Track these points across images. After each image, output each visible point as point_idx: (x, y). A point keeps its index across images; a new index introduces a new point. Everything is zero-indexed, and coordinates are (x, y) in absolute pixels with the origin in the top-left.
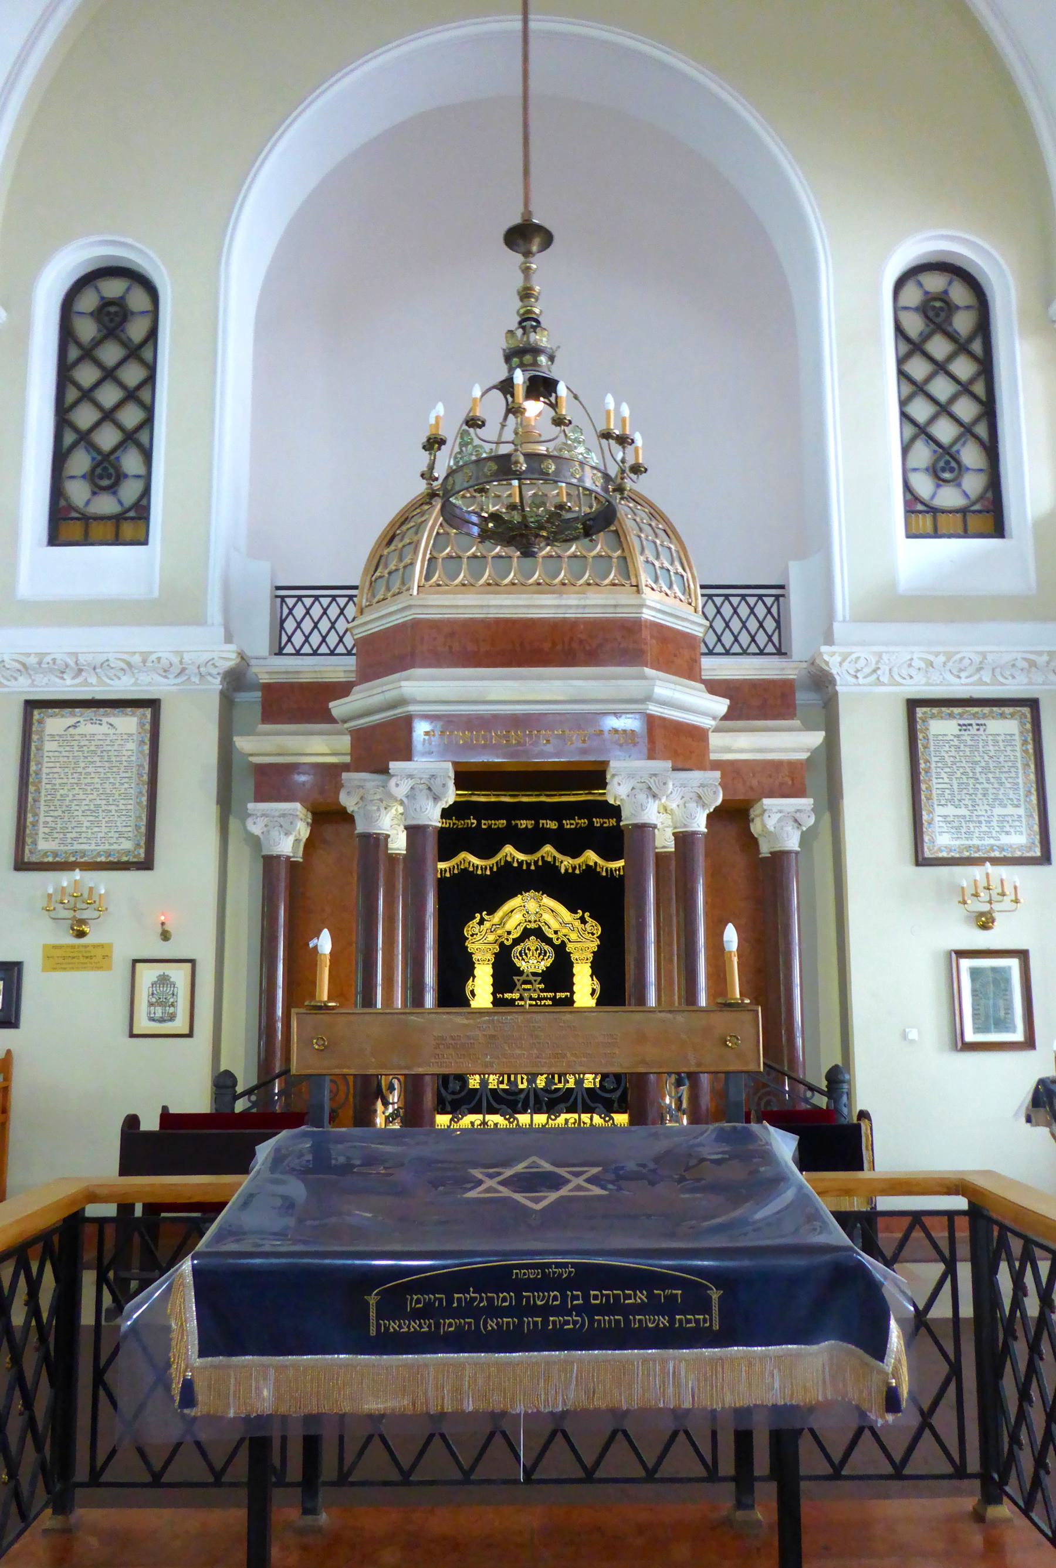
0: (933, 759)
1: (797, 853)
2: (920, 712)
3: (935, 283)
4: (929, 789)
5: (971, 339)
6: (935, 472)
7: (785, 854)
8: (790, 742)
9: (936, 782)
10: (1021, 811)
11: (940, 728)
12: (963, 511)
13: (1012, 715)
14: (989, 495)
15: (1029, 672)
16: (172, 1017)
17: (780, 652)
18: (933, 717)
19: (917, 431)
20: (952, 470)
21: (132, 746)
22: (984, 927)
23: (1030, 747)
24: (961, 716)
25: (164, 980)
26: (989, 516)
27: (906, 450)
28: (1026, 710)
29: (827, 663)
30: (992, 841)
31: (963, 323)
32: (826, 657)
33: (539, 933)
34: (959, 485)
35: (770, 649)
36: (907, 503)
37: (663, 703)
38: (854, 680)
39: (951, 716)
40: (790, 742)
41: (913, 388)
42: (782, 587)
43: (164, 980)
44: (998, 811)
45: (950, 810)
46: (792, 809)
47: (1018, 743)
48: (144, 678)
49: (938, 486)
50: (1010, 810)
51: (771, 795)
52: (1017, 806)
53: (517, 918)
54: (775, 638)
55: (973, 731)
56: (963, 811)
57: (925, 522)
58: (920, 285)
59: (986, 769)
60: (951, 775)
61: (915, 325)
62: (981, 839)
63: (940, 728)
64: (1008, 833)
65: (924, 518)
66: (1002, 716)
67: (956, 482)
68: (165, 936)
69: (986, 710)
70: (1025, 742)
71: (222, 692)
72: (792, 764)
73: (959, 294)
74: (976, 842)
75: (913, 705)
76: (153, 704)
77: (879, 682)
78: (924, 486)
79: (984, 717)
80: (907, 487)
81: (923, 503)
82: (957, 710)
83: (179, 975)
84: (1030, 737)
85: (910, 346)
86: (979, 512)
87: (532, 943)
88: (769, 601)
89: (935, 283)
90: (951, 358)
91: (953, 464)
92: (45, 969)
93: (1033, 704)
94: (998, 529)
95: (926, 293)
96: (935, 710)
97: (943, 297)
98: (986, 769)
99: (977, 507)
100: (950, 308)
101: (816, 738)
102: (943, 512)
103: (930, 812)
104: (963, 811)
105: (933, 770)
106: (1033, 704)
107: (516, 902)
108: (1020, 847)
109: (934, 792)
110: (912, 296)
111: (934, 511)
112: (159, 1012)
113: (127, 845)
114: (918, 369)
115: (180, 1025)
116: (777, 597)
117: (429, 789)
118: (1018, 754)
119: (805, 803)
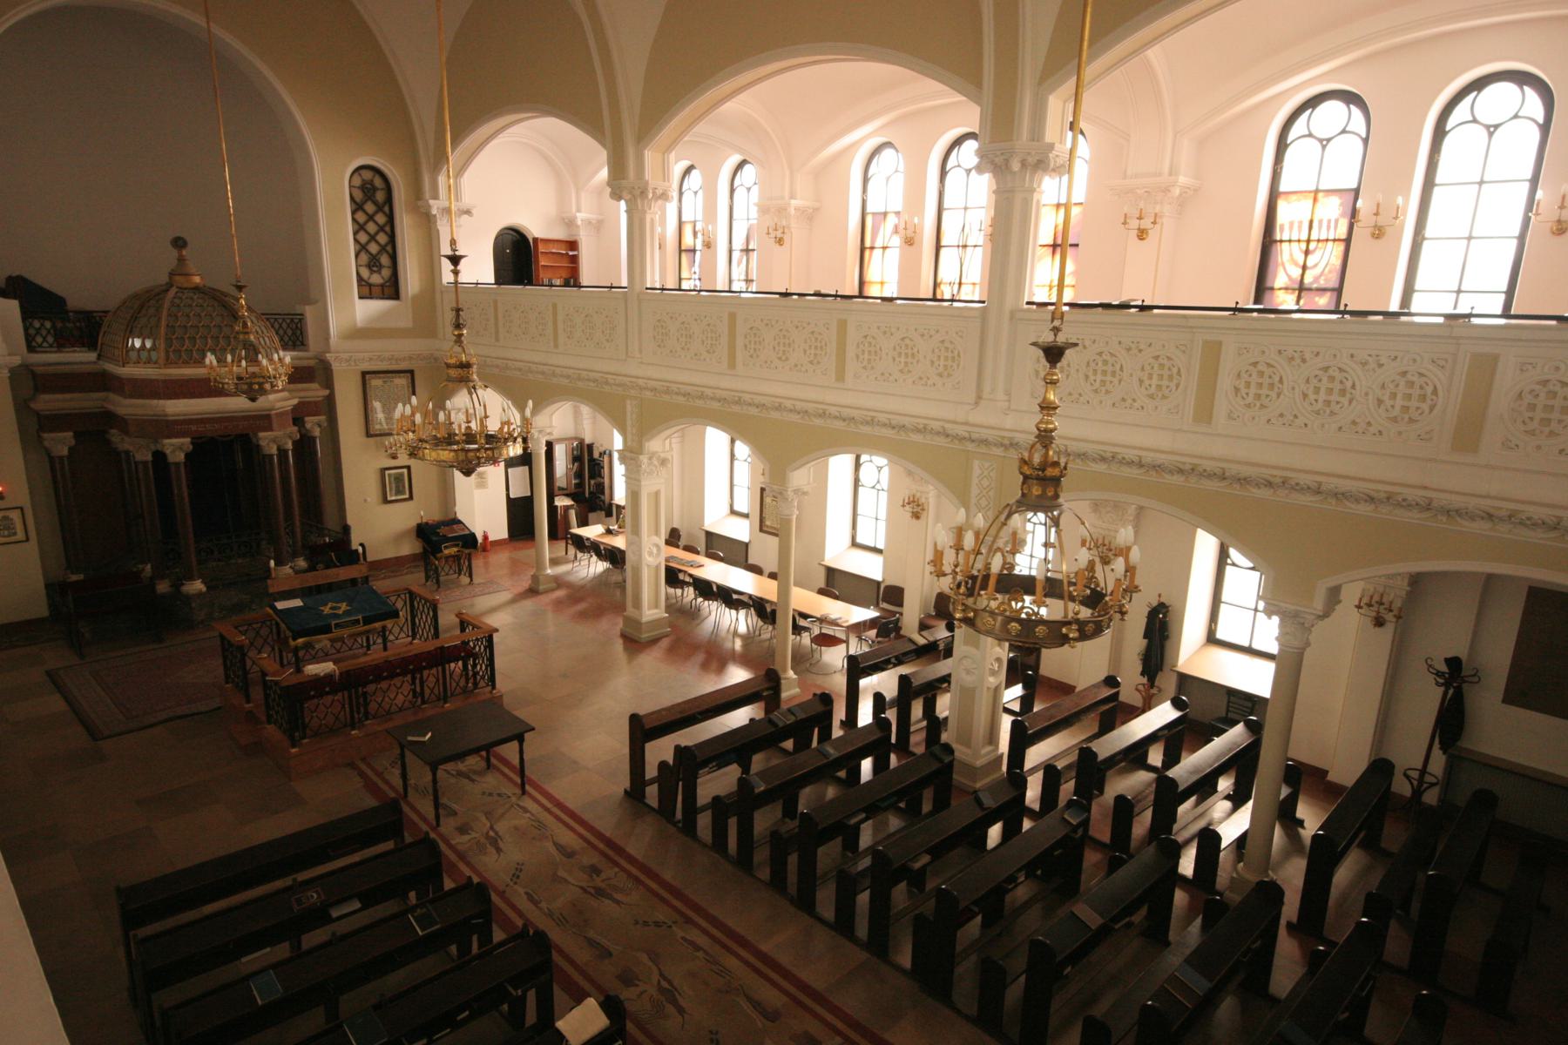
0: (370, 393)
3: (367, 175)
8: (315, 392)
11: (375, 382)
26: (391, 289)
31: (380, 196)
40: (315, 392)
41: (359, 228)
61: (359, 195)
63: (375, 382)
72: (316, 403)
73: (378, 182)
75: (364, 374)
83: (15, 516)
89: (367, 175)
93: (411, 372)
94: (396, 296)
100: (375, 189)
106: (411, 372)
110: (357, 181)
111: (370, 285)
114: (361, 217)
115: (20, 535)
119: (323, 418)
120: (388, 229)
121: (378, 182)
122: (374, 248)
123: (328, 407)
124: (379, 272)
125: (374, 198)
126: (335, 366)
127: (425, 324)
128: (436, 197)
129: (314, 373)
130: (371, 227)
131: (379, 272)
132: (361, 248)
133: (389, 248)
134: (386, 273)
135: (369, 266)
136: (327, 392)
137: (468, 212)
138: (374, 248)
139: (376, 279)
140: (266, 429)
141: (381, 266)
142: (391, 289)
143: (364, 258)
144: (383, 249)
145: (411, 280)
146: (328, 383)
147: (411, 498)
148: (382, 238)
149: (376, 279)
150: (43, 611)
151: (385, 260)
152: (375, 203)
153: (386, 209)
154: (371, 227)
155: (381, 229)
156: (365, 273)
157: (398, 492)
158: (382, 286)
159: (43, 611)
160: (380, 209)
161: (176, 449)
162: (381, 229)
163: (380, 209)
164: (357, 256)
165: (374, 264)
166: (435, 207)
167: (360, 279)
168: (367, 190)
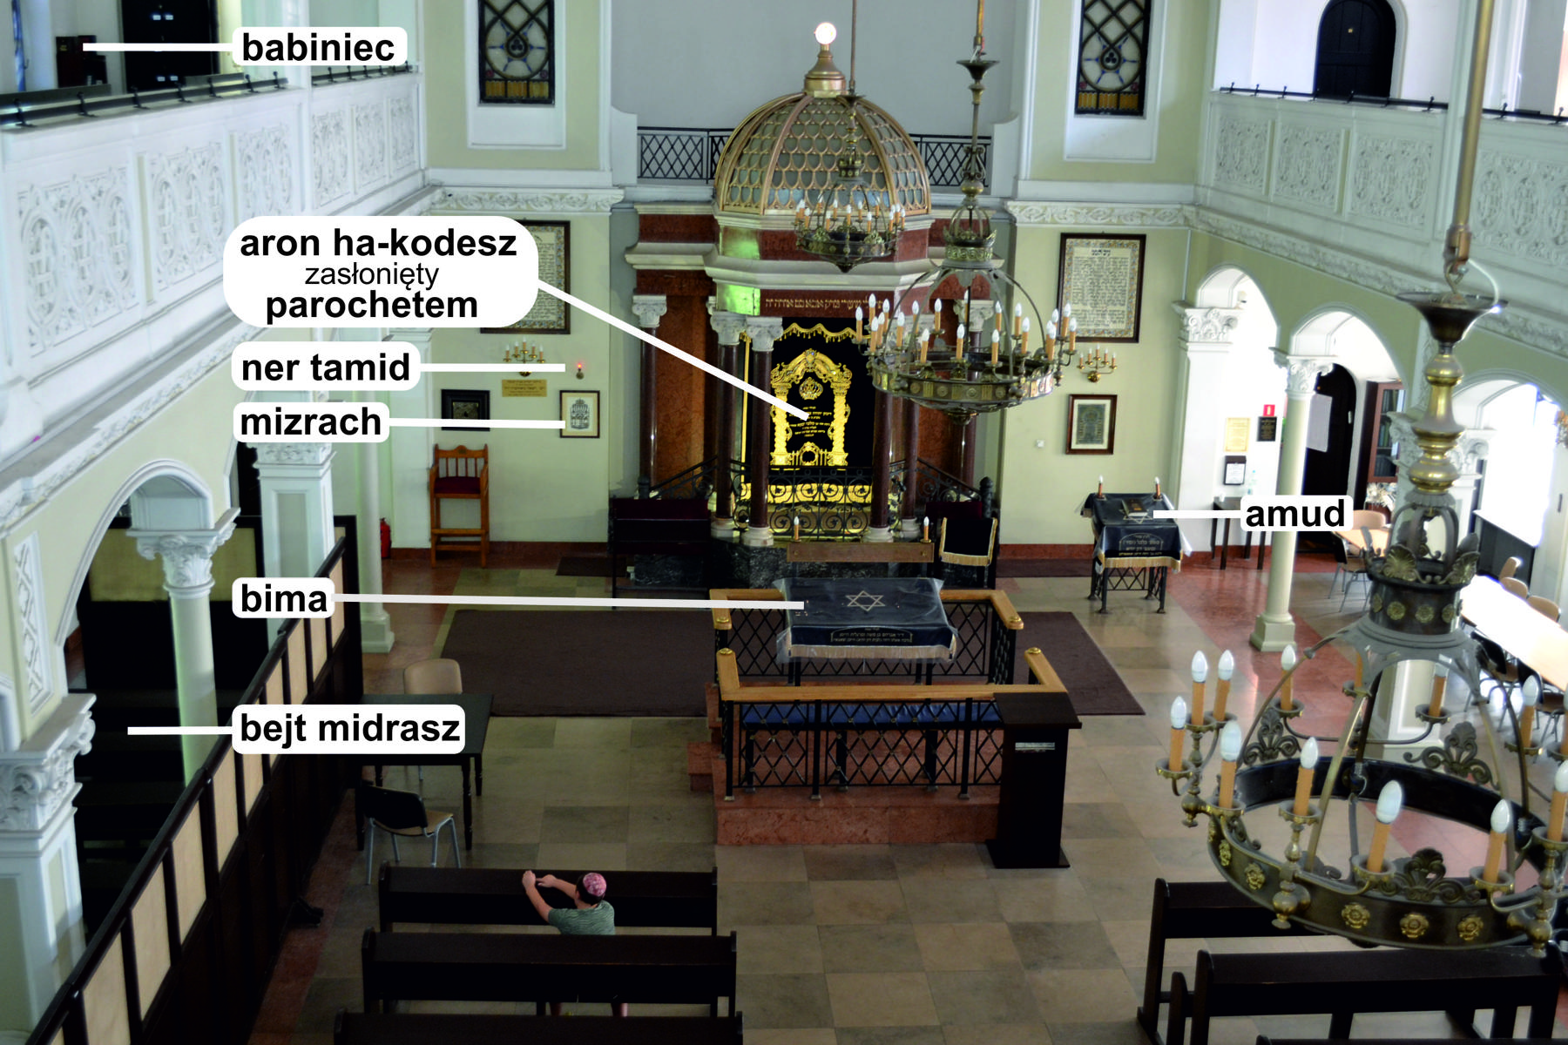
16: (586, 426)
21: (553, 252)
22: (1093, 380)
25: (580, 403)
26: (1131, 101)
33: (813, 376)
43: (580, 403)
44: (1111, 308)
47: (1129, 264)
48: (558, 206)
50: (1118, 307)
53: (802, 366)
65: (1091, 101)
68: (580, 376)
75: (1065, 236)
76: (566, 225)
77: (1044, 222)
83: (590, 400)
87: (809, 381)
92: (504, 395)
94: (1138, 110)
98: (1106, 281)
106: (1142, 238)
107: (800, 358)
111: (1099, 91)
112: (578, 422)
113: (553, 318)
115: (591, 430)
122: (1113, 30)
124: (1116, 69)
127: (1176, 163)
131: (1116, 69)
132: (1092, 30)
134: (1128, 71)
135: (1101, 60)
138: (1113, 30)
139: (1110, 81)
142: (1131, 101)
143: (1095, 47)
144: (1128, 31)
147: (1110, 450)
150: (602, 536)
151: (1129, 50)
156: (1093, 71)
157: (1089, 438)
158: (1118, 92)
159: (602, 536)
164: (1082, 45)
165: (1110, 58)
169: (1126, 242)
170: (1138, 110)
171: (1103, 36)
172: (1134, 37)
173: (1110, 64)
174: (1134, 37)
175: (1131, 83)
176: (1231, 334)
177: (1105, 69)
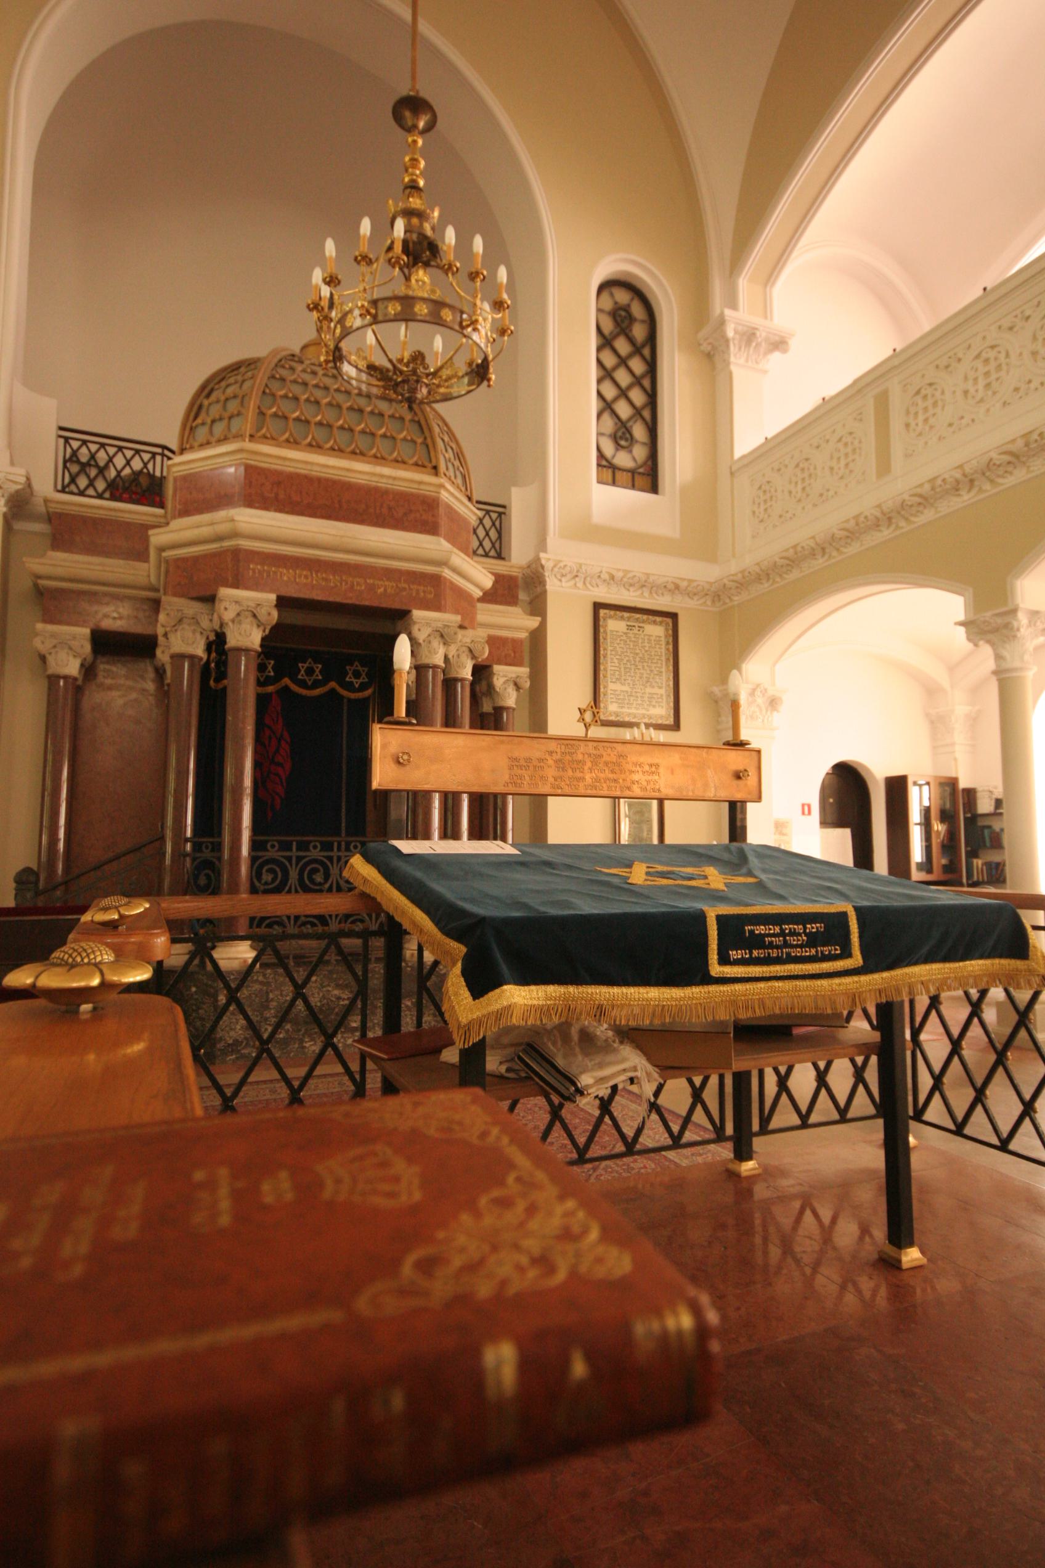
0: (608, 647)
1: (514, 709)
2: (602, 612)
3: (622, 296)
4: (605, 670)
5: (643, 346)
6: (615, 438)
7: (507, 708)
9: (609, 665)
10: (662, 691)
11: (614, 625)
12: (633, 472)
13: (661, 623)
14: (650, 463)
15: (673, 593)
17: (500, 556)
18: (611, 617)
19: (607, 407)
20: (626, 440)
23: (671, 647)
24: (629, 619)
26: (649, 477)
27: (599, 415)
28: (669, 621)
29: (543, 567)
30: (644, 712)
31: (639, 332)
32: (543, 562)
34: (631, 452)
35: (492, 553)
36: (598, 458)
37: (455, 570)
38: (558, 583)
39: (622, 618)
41: (606, 374)
42: (504, 507)
44: (648, 690)
45: (617, 687)
46: (514, 676)
47: (663, 642)
49: (617, 450)
50: (656, 690)
51: (499, 663)
52: (660, 688)
54: (497, 545)
55: (636, 631)
56: (626, 688)
57: (608, 474)
58: (612, 295)
59: (642, 660)
60: (620, 660)
61: (608, 326)
62: (637, 709)
63: (614, 625)
64: (654, 706)
66: (655, 622)
67: (629, 449)
69: (645, 617)
70: (668, 643)
71: (5, 515)
72: (514, 642)
73: (637, 310)
74: (633, 711)
75: (597, 606)
78: (609, 449)
79: (643, 622)
80: (599, 449)
81: (607, 460)
82: (626, 615)
84: (671, 640)
85: (605, 342)
86: (643, 474)
88: (494, 516)
90: (630, 356)
91: (628, 436)
93: (674, 616)
94: (654, 488)
95: (616, 303)
96: (612, 613)
97: (626, 309)
98: (642, 660)
99: (641, 470)
100: (631, 319)
101: (534, 622)
102: (620, 469)
103: (605, 687)
104: (626, 688)
105: (609, 656)
106: (674, 616)
108: (661, 717)
109: (609, 672)
110: (608, 304)
116: (500, 514)
117: (255, 616)
118: (663, 650)
120: (646, 383)
121: (637, 310)
123: (533, 651)
125: (629, 325)
126: (552, 585)
127: (702, 532)
128: (734, 306)
129: (522, 589)
130: (623, 378)
133: (646, 414)
134: (640, 453)
136: (534, 622)
137: (779, 344)
138: (623, 410)
140: (427, 606)
141: (632, 440)
142: (649, 477)
144: (638, 412)
145: (679, 456)
146: (538, 606)
148: (638, 397)
149: (623, 460)
151: (639, 431)
152: (631, 340)
153: (646, 352)
154: (623, 378)
155: (637, 381)
160: (637, 350)
161: (246, 616)
162: (637, 381)
163: (637, 350)
165: (622, 436)
166: (736, 320)
167: (601, 455)
168: (621, 318)
169: (658, 619)
170: (654, 488)
171: (614, 413)
172: (643, 419)
173: (623, 443)
174: (643, 419)
175: (645, 463)
176: (777, 718)
177: (618, 447)
